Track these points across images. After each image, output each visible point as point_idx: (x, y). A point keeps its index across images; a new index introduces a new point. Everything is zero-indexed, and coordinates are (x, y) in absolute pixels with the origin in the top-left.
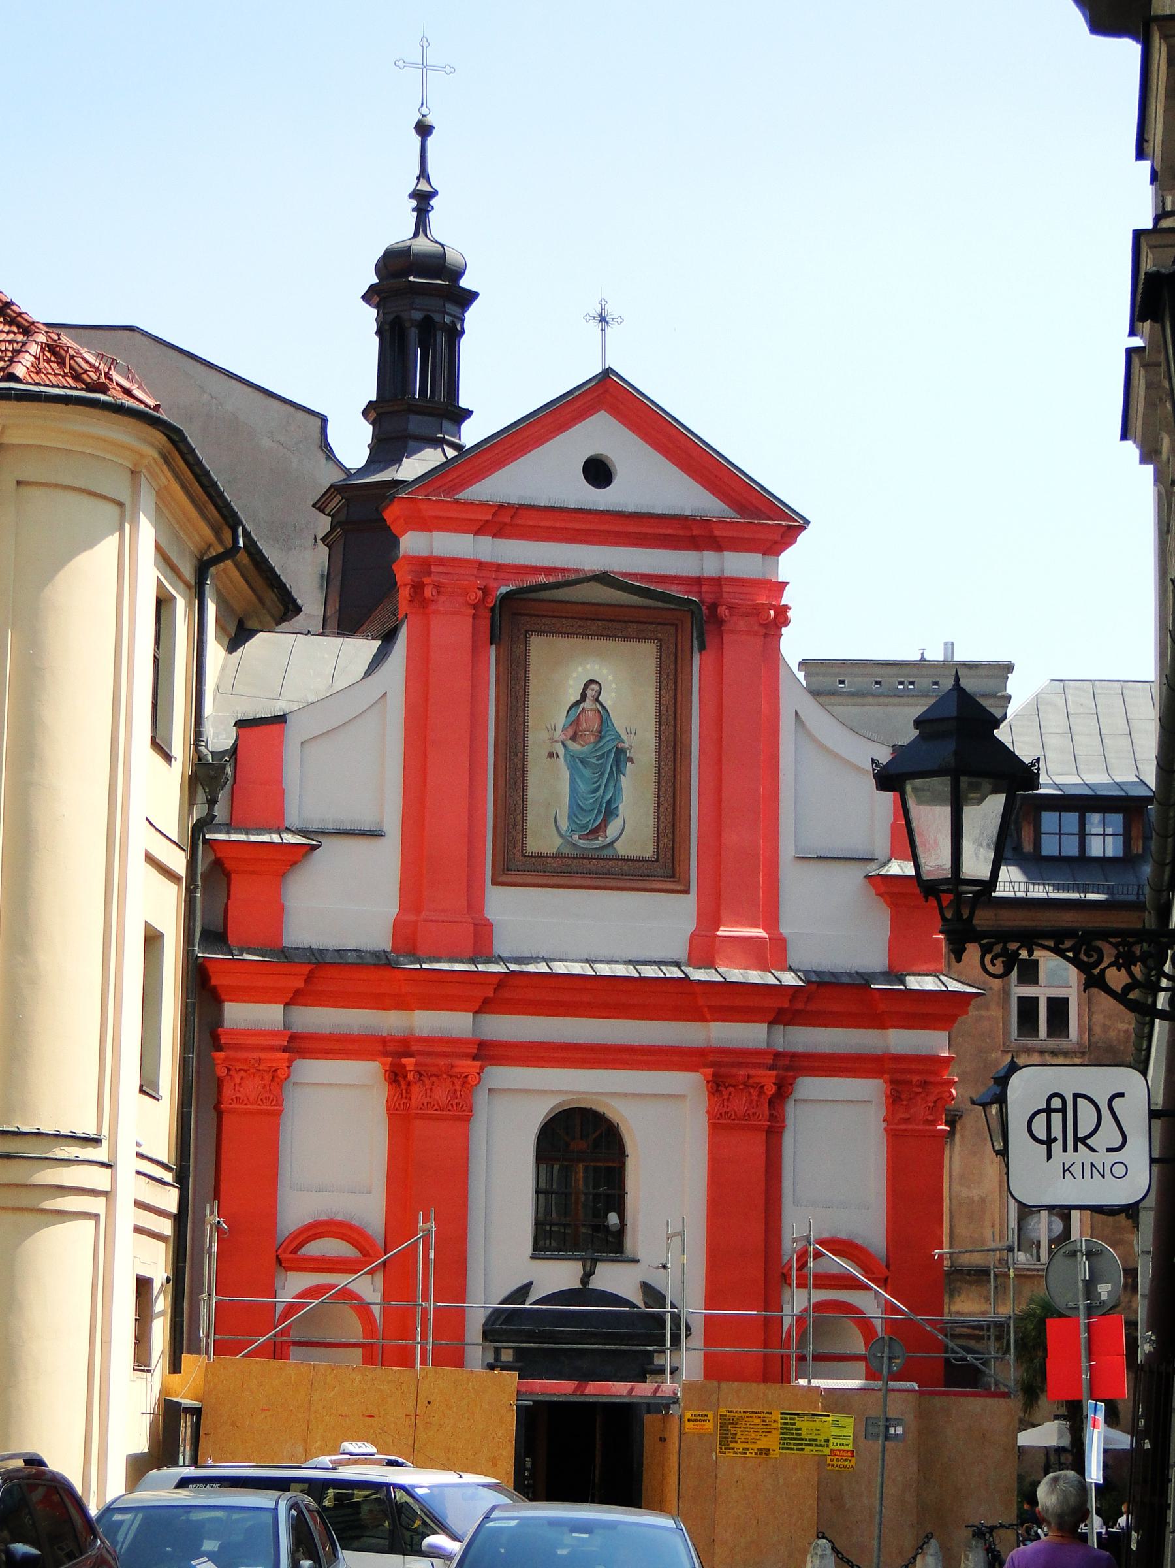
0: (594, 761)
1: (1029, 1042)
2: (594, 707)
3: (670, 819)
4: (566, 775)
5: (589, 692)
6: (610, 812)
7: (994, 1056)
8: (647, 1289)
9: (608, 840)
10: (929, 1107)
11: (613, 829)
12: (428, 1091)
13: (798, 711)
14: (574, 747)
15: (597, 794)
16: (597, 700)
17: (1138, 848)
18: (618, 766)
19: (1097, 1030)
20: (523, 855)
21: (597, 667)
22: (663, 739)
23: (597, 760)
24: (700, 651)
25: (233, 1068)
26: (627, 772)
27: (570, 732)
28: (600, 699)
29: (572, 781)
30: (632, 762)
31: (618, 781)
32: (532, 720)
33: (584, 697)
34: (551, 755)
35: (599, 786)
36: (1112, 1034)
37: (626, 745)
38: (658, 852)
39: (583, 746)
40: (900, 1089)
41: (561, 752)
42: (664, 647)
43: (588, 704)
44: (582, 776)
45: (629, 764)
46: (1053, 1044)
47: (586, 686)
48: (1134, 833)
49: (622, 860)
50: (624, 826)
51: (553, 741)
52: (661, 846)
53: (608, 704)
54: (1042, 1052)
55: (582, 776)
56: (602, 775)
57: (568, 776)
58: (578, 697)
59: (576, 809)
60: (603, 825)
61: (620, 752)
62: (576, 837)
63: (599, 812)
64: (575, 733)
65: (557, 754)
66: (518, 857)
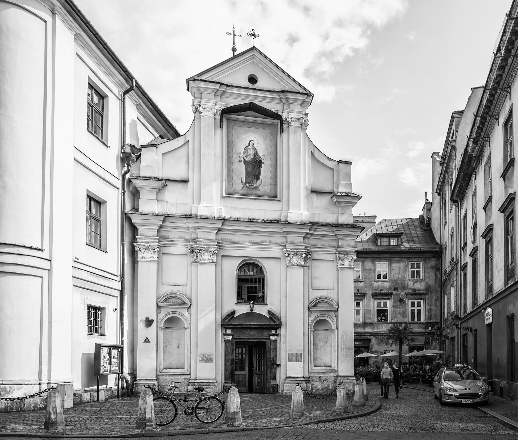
1: (379, 280)
7: (372, 282)
17: (400, 243)
19: (392, 277)
31: (260, 169)
36: (395, 278)
45: (263, 165)
46: (384, 280)
48: (399, 241)
54: (382, 281)
61: (261, 161)
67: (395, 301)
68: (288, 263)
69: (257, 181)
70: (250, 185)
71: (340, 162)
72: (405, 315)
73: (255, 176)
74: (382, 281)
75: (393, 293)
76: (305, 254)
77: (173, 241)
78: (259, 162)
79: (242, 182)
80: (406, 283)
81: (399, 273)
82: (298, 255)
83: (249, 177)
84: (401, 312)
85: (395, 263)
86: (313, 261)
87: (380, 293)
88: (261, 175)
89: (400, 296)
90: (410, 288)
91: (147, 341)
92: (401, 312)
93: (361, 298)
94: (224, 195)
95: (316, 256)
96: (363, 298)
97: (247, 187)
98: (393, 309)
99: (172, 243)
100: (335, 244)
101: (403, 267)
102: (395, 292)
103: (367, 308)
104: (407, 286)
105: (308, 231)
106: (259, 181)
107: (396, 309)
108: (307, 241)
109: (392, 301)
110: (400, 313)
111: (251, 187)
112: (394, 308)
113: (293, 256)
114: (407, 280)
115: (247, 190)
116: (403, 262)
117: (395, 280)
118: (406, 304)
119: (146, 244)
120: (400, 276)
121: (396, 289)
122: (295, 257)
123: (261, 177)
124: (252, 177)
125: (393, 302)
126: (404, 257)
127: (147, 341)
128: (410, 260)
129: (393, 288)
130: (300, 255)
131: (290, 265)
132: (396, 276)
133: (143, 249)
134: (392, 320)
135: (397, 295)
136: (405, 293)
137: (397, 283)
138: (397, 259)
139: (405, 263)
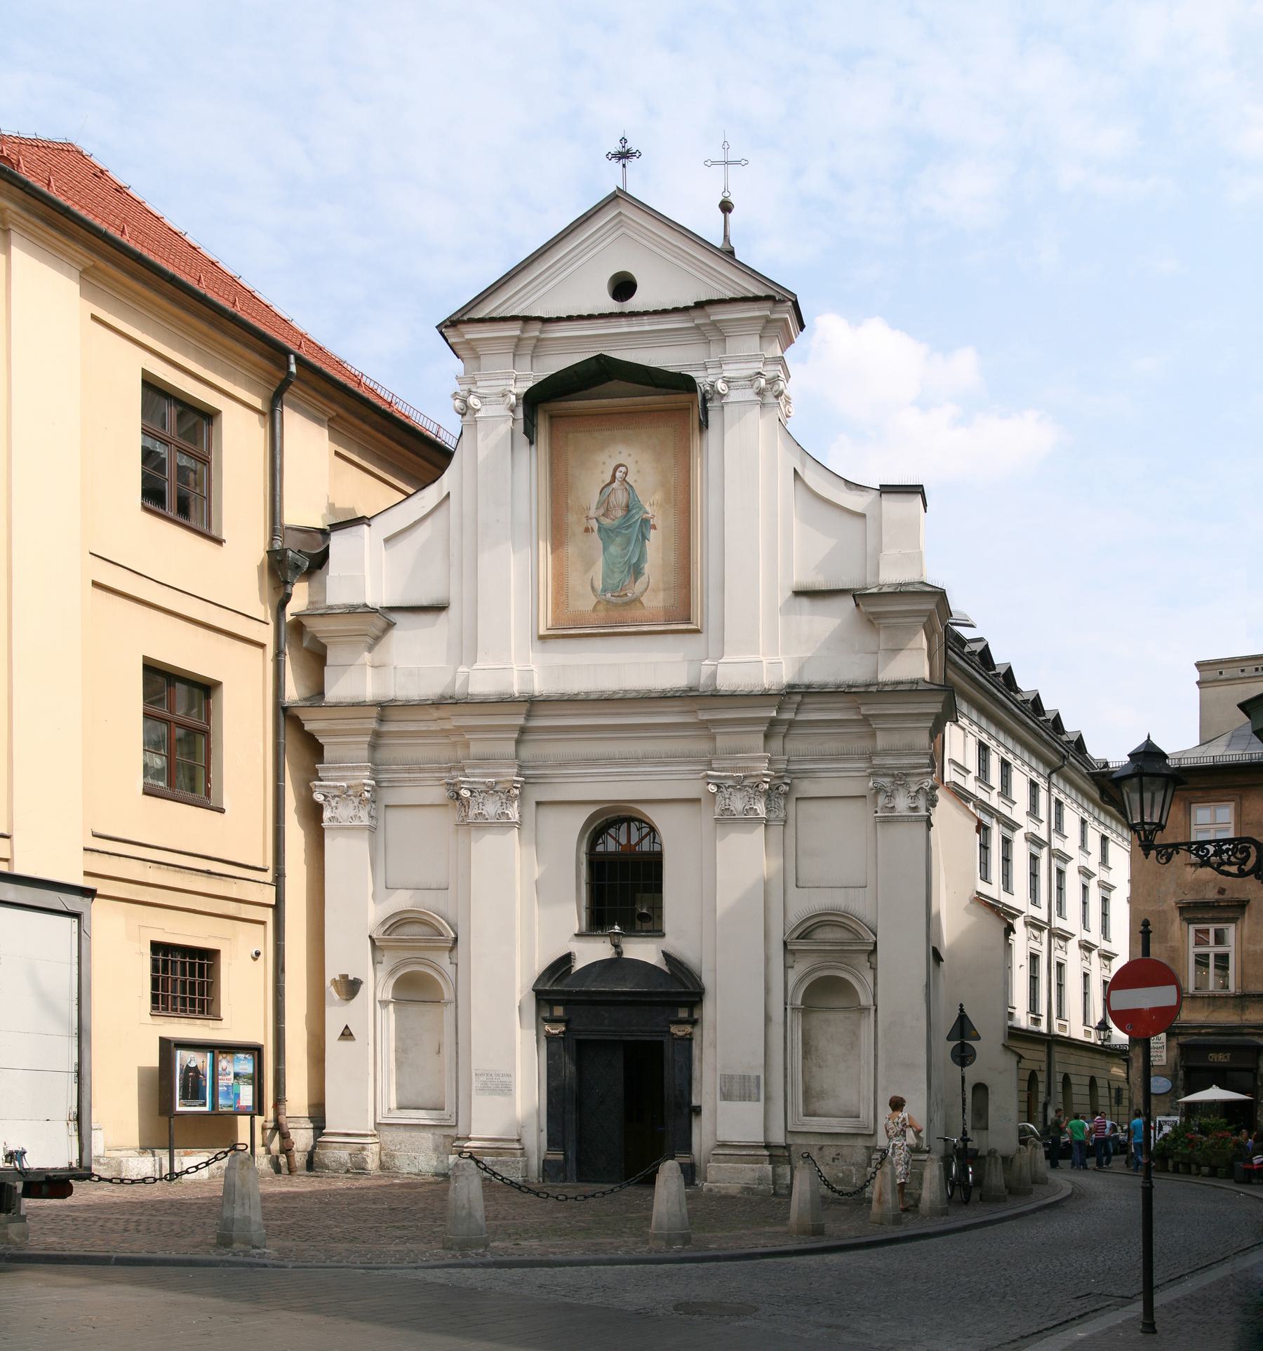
5: (618, 474)
8: (667, 956)
12: (481, 805)
16: (624, 479)
23: (627, 529)
27: (602, 511)
30: (654, 527)
33: (614, 477)
34: (587, 530)
37: (650, 515)
41: (595, 526)
50: (649, 582)
57: (602, 546)
58: (608, 481)
62: (609, 595)
64: (607, 510)
65: (592, 528)
68: (717, 810)
69: (636, 581)
70: (616, 594)
73: (629, 568)
77: (409, 771)
78: (641, 526)
79: (593, 588)
83: (613, 572)
86: (802, 805)
88: (646, 562)
91: (347, 1034)
93: (1231, 915)
94: (542, 632)
95: (807, 788)
96: (1236, 915)
97: (608, 602)
99: (407, 775)
100: (864, 745)
103: (1252, 948)
106: (642, 580)
108: (776, 744)
111: (619, 600)
113: (730, 790)
115: (607, 610)
119: (339, 784)
122: (739, 795)
123: (647, 567)
124: (623, 572)
127: (347, 1034)
130: (751, 788)
131: (727, 820)
133: (335, 796)
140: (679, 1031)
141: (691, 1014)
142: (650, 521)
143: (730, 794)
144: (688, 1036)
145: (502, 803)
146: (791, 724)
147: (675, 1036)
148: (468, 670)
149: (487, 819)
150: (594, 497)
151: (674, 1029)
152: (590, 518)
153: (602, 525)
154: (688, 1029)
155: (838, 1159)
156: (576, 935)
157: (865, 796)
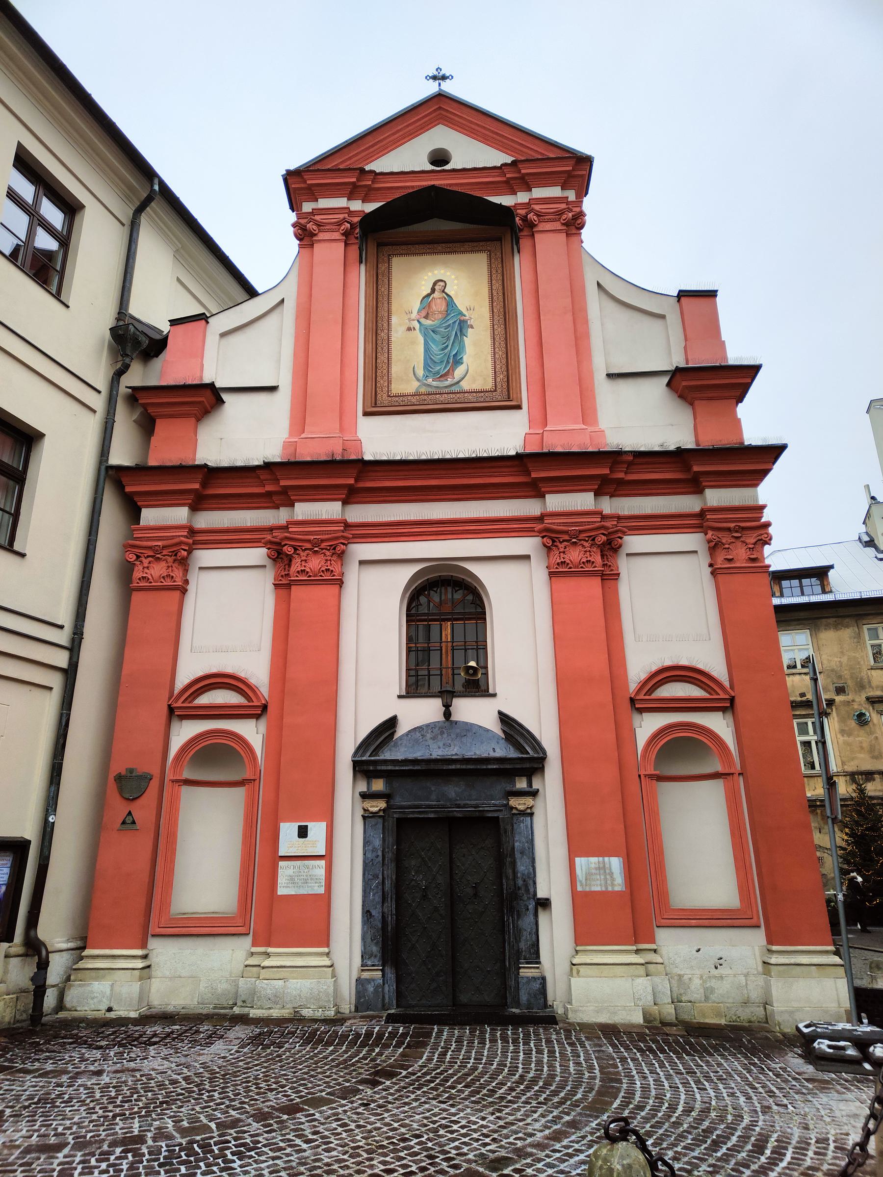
0: (442, 330)
2: (441, 296)
3: (504, 361)
4: (421, 340)
5: (437, 287)
6: (457, 361)
8: (504, 719)
9: (455, 380)
10: (750, 548)
11: (459, 372)
13: (600, 282)
14: (428, 322)
15: (446, 351)
16: (443, 291)
18: (461, 331)
19: (825, 662)
20: (389, 396)
21: (442, 271)
22: (495, 311)
24: (519, 252)
25: (142, 555)
26: (469, 335)
27: (424, 313)
28: (446, 290)
29: (426, 344)
30: (472, 327)
32: (394, 307)
33: (433, 290)
35: (447, 346)
37: (467, 318)
38: (495, 385)
39: (433, 321)
40: (720, 536)
41: (417, 326)
42: (493, 254)
43: (436, 295)
44: (434, 340)
47: (435, 284)
49: (467, 392)
51: (410, 320)
52: (498, 380)
53: (452, 293)
55: (434, 340)
56: (448, 339)
57: (423, 341)
58: (429, 291)
59: (429, 362)
60: (451, 371)
63: (448, 362)
66: (385, 396)
67: (842, 720)
71: (683, 295)
72: (876, 753)
74: (800, 674)
75: (834, 700)
76: (603, 534)
80: (864, 674)
81: (842, 652)
82: (580, 540)
84: (865, 745)
85: (826, 629)
87: (802, 702)
89: (856, 707)
90: (877, 687)
92: (865, 745)
98: (841, 739)
101: (850, 638)
102: (839, 699)
104: (869, 682)
105: (606, 471)
107: (851, 739)
109: (836, 719)
110: (862, 748)
112: (843, 736)
114: (865, 668)
116: (847, 626)
117: (833, 670)
118: (874, 724)
120: (844, 660)
121: (840, 690)
123: (467, 358)
125: (838, 722)
126: (848, 616)
128: (865, 622)
129: (832, 688)
132: (836, 659)
134: (846, 767)
135: (848, 703)
136: (868, 699)
137: (840, 677)
138: (831, 621)
139: (851, 628)
140: (519, 804)
141: (530, 784)
142: (467, 322)
143: (565, 548)
144: (529, 811)
145: (327, 560)
146: (621, 483)
147: (514, 811)
148: (296, 440)
149: (310, 576)
150: (416, 305)
151: (514, 802)
152: (414, 320)
153: (423, 325)
154: (529, 801)
155: (721, 965)
156: (400, 697)
157: (696, 552)
